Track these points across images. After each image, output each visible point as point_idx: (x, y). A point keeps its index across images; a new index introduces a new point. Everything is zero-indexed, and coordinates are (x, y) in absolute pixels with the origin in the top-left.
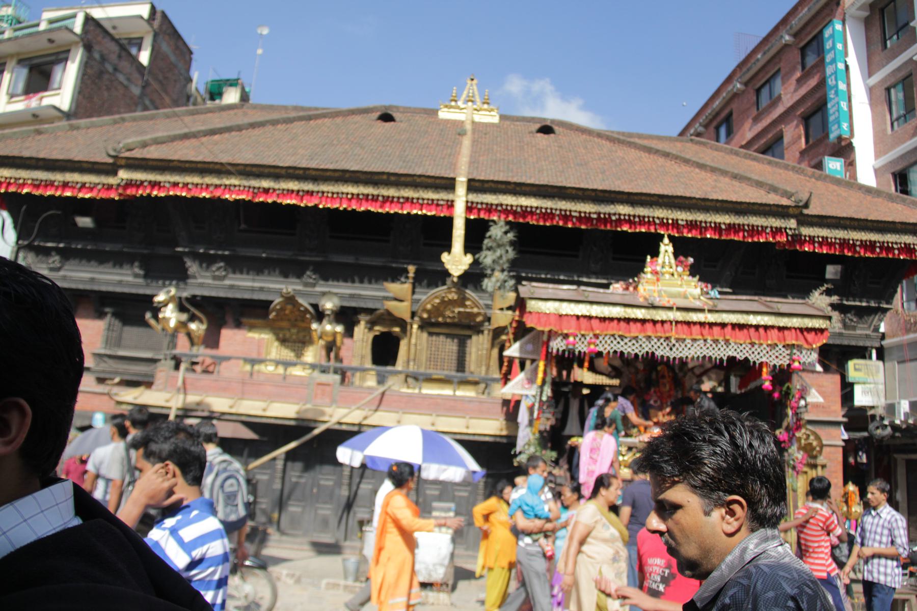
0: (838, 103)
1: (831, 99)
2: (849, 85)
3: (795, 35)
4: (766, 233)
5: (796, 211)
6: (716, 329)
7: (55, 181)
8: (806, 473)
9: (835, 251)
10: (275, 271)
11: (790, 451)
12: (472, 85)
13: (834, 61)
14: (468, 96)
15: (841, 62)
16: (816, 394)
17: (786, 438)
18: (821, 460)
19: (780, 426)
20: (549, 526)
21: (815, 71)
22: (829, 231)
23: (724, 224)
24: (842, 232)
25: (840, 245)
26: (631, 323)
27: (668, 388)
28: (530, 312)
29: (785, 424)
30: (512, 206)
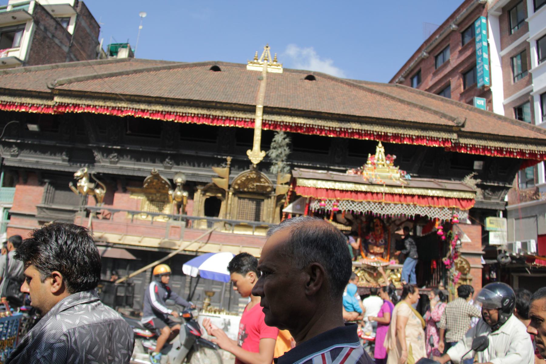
0: (483, 66)
1: (479, 63)
2: (489, 55)
3: (459, 25)
5: (457, 129)
6: (409, 198)
7: (15, 103)
9: (480, 153)
10: (185, 163)
11: (451, 270)
12: (267, 50)
13: (481, 41)
14: (265, 57)
15: (485, 41)
17: (449, 263)
18: (469, 276)
19: (445, 256)
20: (360, 317)
21: (470, 46)
25: (483, 149)
27: (380, 231)
28: (299, 186)
29: (448, 255)
30: (289, 123)
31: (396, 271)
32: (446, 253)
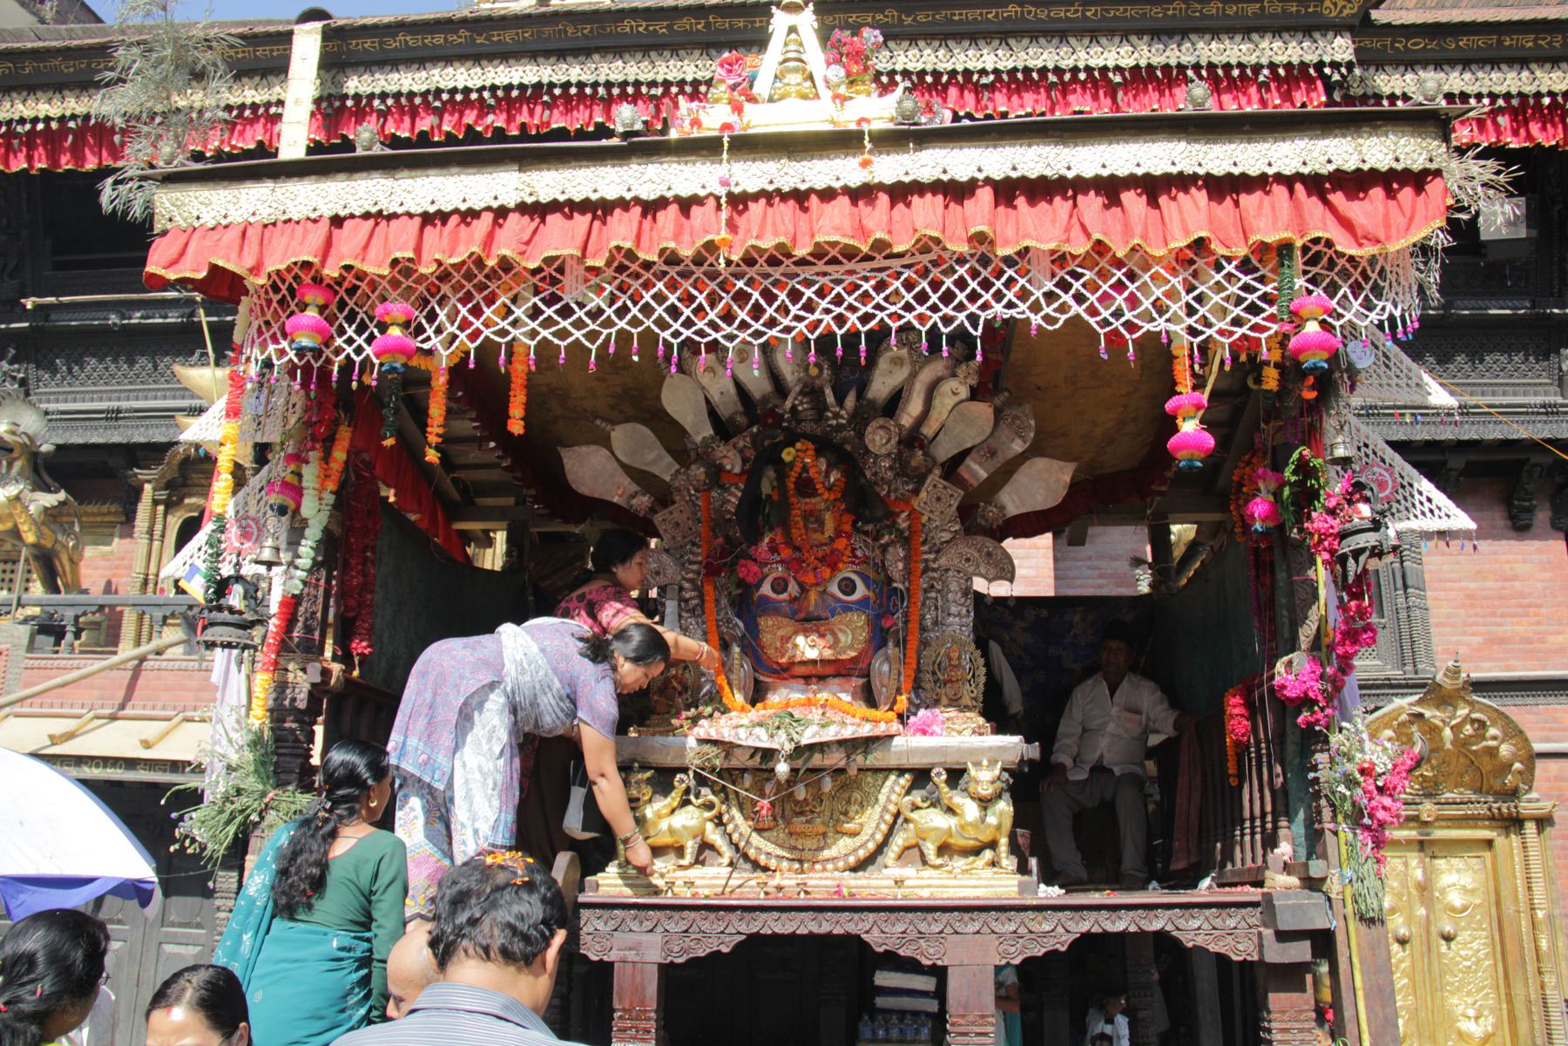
4: (1260, 86)
11: (1335, 739)
16: (1440, 498)
18: (1529, 805)
19: (1293, 646)
22: (1467, 76)
23: (1118, 69)
24: (1512, 75)
25: (1515, 113)
26: (554, 219)
28: (164, 233)
29: (1306, 633)
30: (467, 91)
31: (940, 777)
32: (1297, 621)
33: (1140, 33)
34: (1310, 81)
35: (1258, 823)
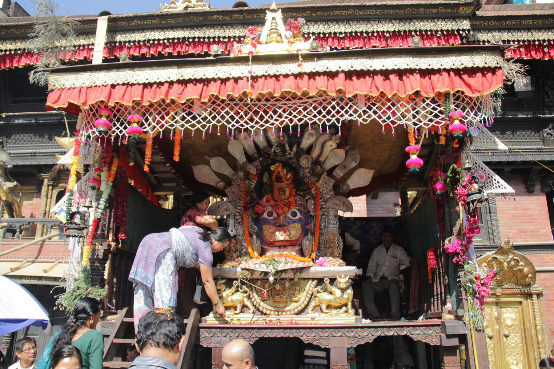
4: (438, 38)
5: (468, 11)
8: (520, 303)
9: (521, 56)
11: (466, 267)
16: (502, 182)
18: (535, 288)
19: (451, 234)
22: (510, 34)
23: (388, 32)
24: (525, 34)
25: (526, 47)
26: (190, 86)
28: (52, 91)
29: (456, 229)
30: (159, 40)
31: (327, 281)
32: (452, 225)
33: (395, 19)
34: (455, 36)
35: (439, 296)
